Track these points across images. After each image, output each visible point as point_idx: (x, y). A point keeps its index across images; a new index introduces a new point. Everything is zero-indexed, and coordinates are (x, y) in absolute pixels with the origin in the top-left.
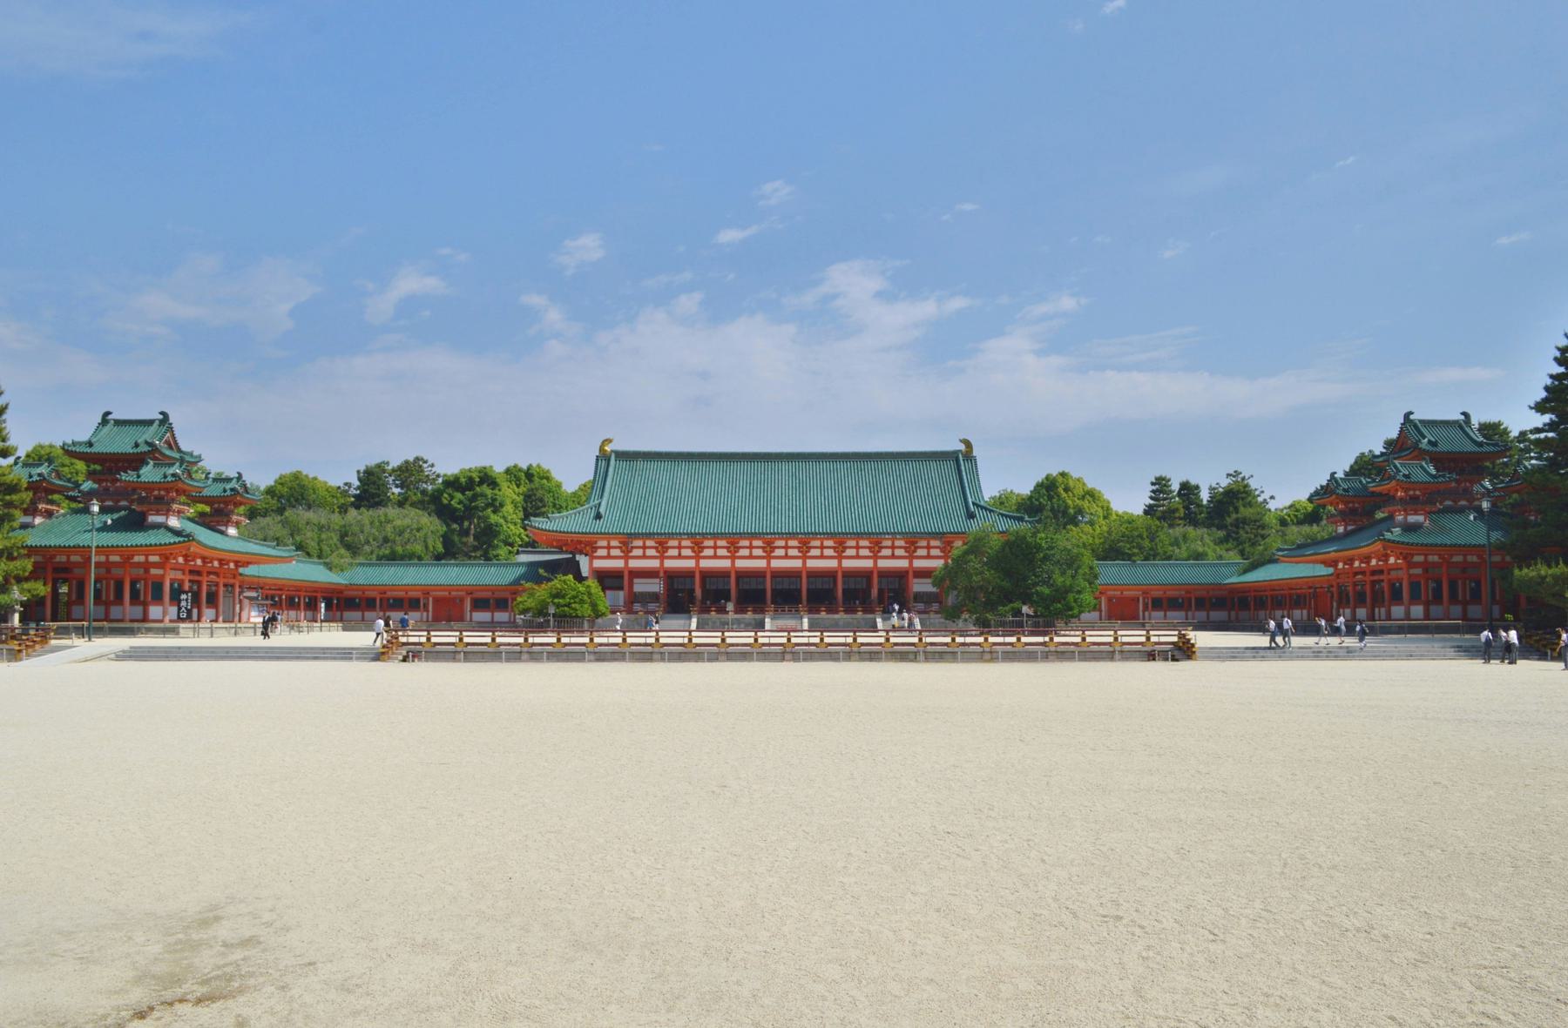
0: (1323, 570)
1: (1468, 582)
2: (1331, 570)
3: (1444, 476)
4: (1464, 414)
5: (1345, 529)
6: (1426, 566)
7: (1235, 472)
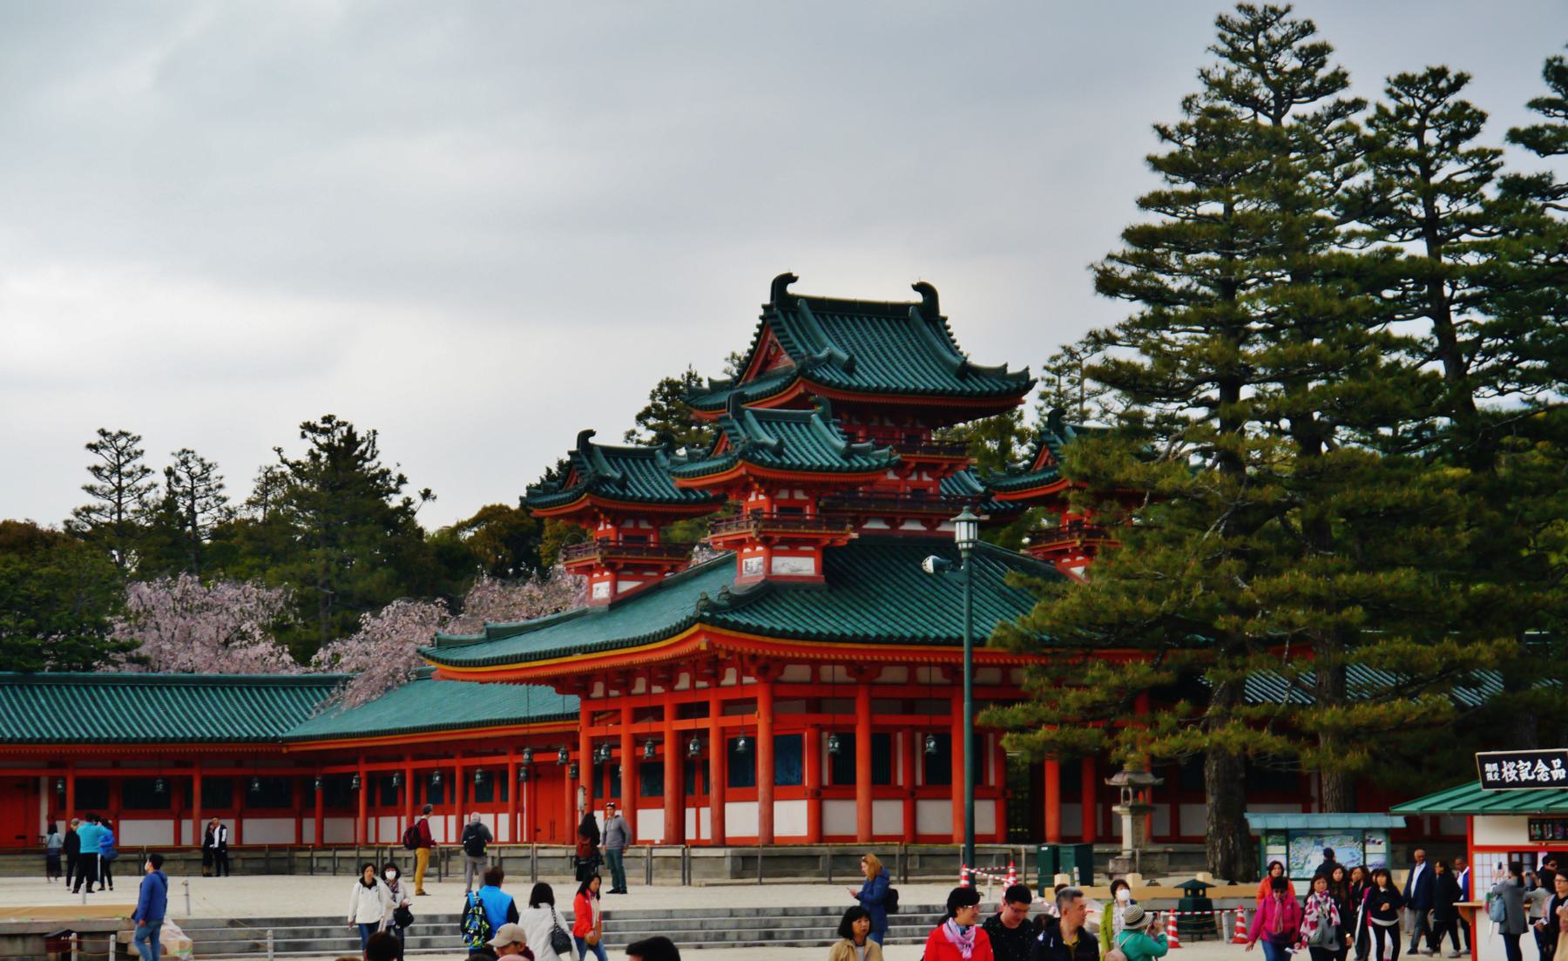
0: (548, 702)
1: (919, 736)
2: (572, 703)
3: (864, 453)
4: (922, 288)
5: (614, 587)
6: (816, 699)
7: (328, 419)
